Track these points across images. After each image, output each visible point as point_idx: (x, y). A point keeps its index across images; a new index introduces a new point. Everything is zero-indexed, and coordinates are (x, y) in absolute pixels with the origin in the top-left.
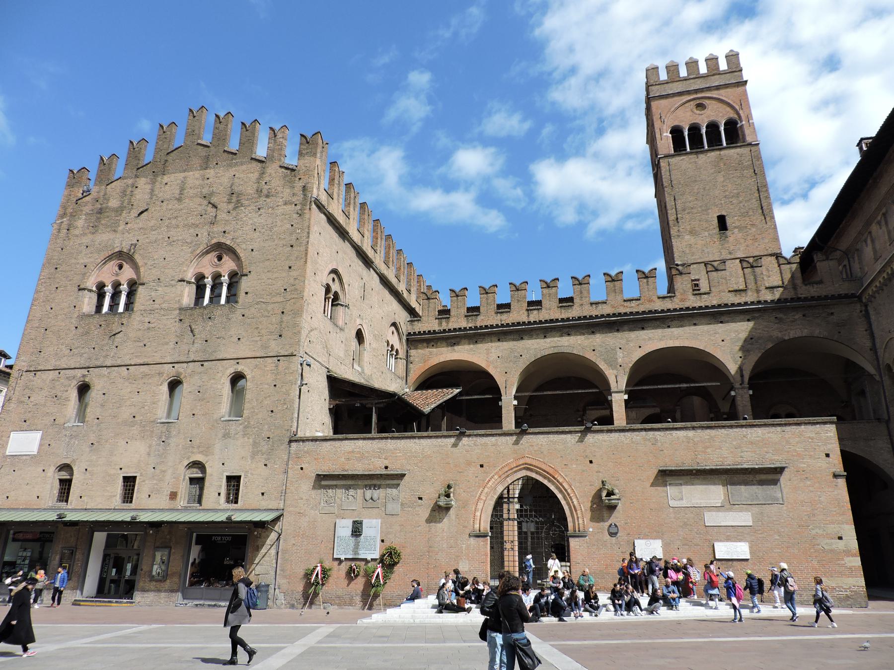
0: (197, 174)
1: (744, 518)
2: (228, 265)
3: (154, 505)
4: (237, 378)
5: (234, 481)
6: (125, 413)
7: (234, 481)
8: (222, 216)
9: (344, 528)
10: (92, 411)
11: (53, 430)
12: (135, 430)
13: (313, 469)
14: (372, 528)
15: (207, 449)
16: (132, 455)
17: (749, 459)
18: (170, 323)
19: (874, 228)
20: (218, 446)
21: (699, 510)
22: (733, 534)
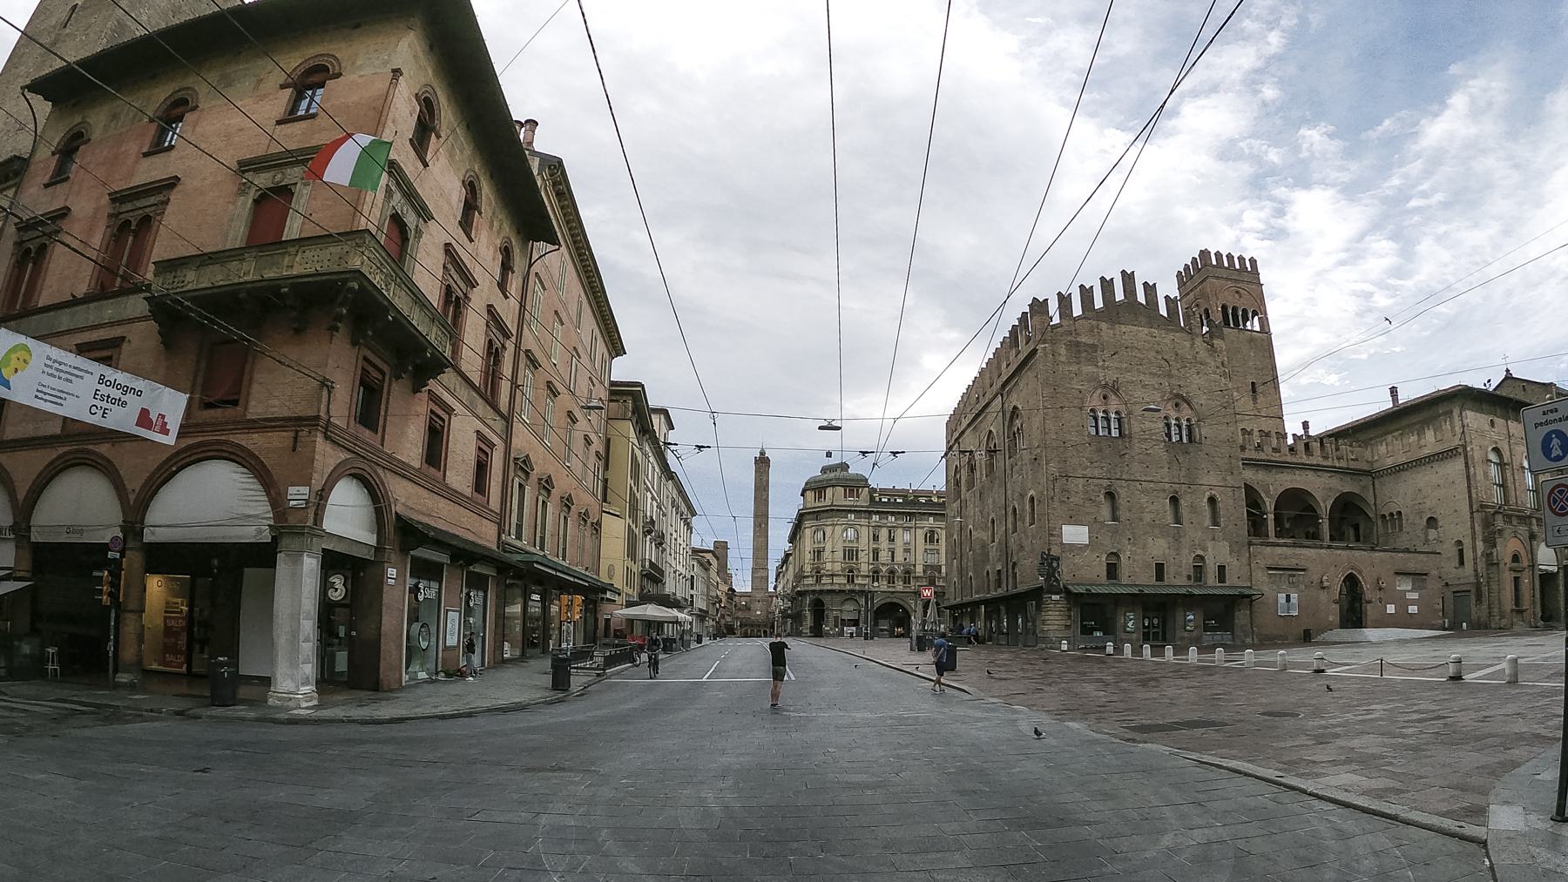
0: (1146, 330)
1: (1415, 596)
2: (1186, 412)
3: (1177, 581)
4: (1212, 500)
5: (1222, 569)
6: (1148, 518)
7: (1222, 569)
8: (1174, 372)
9: (1282, 598)
10: (1123, 514)
11: (1095, 525)
12: (1157, 531)
13: (1263, 563)
14: (1294, 597)
15: (1204, 549)
16: (1158, 548)
17: (1419, 568)
18: (1160, 451)
19: (1389, 438)
20: (1210, 544)
21: (1405, 591)
22: (1413, 602)
